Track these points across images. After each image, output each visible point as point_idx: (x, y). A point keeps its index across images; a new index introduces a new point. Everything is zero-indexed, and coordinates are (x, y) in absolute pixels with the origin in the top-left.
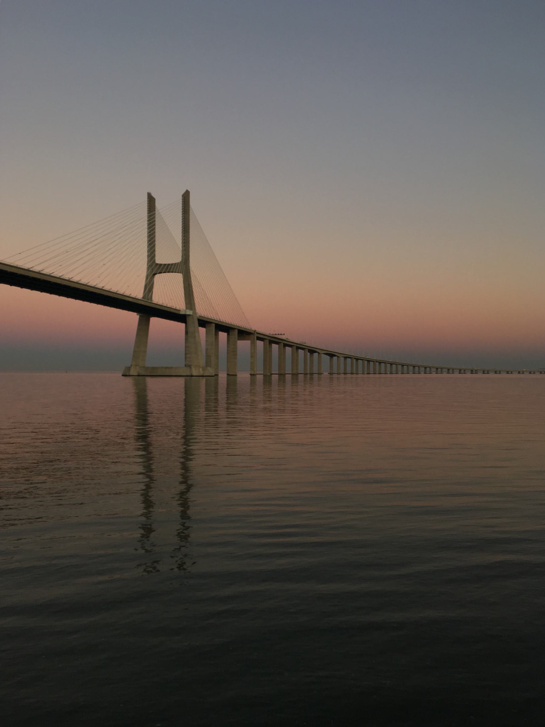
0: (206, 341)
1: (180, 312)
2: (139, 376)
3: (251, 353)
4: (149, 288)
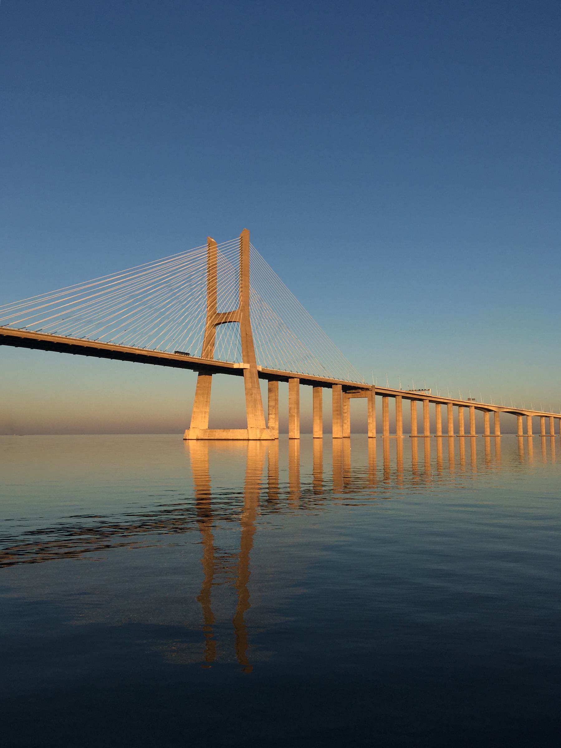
0: (289, 398)
1: (233, 367)
2: (197, 440)
3: (369, 412)
4: (210, 341)
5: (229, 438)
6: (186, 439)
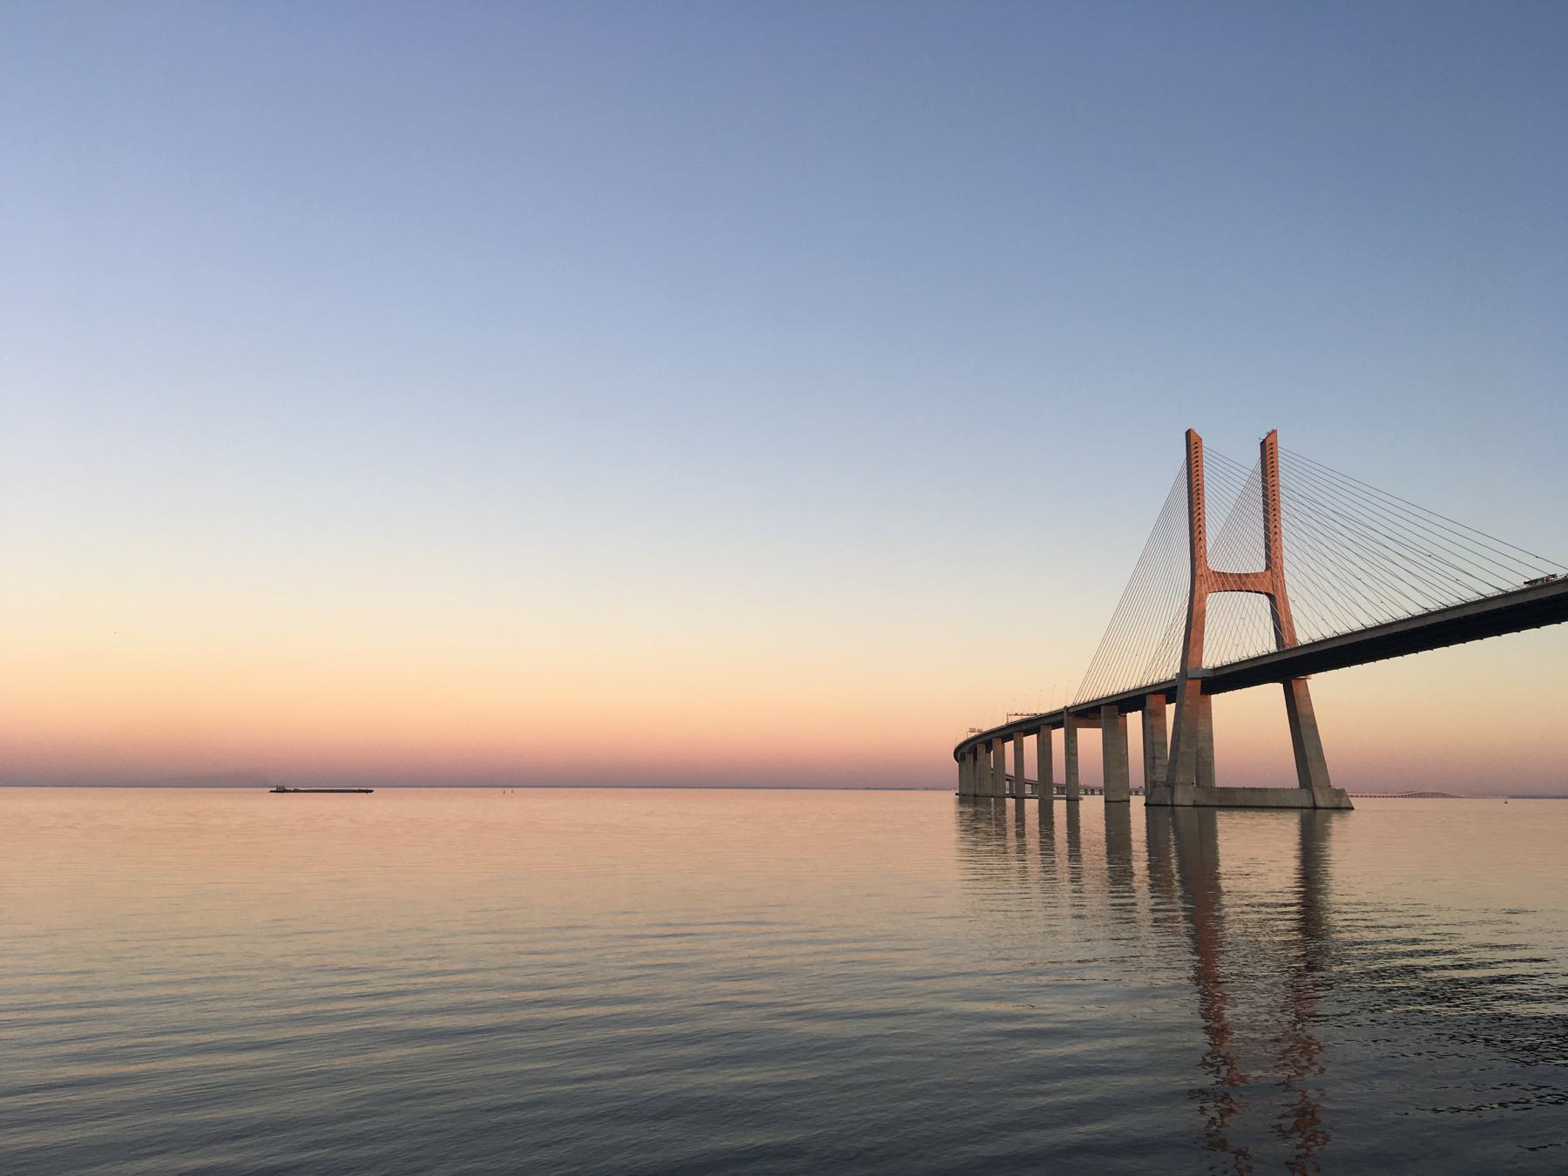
2: (1194, 806)
5: (1270, 804)
6: (1167, 806)
